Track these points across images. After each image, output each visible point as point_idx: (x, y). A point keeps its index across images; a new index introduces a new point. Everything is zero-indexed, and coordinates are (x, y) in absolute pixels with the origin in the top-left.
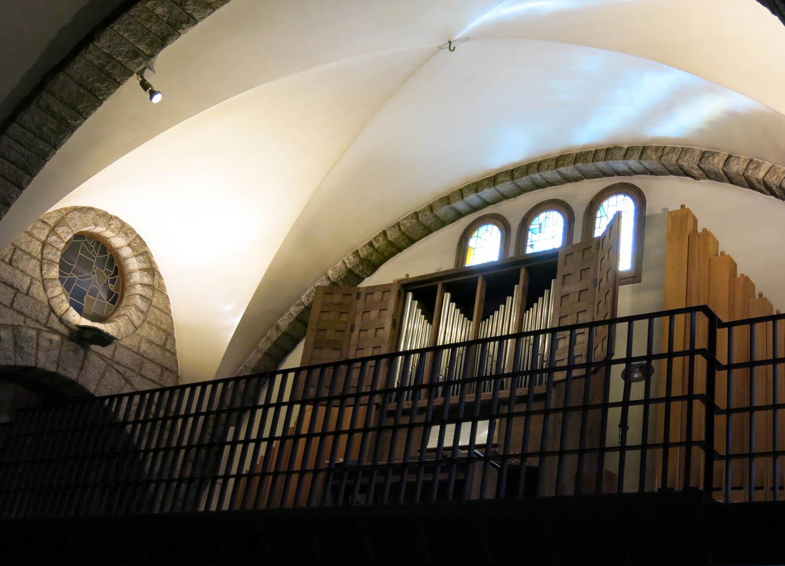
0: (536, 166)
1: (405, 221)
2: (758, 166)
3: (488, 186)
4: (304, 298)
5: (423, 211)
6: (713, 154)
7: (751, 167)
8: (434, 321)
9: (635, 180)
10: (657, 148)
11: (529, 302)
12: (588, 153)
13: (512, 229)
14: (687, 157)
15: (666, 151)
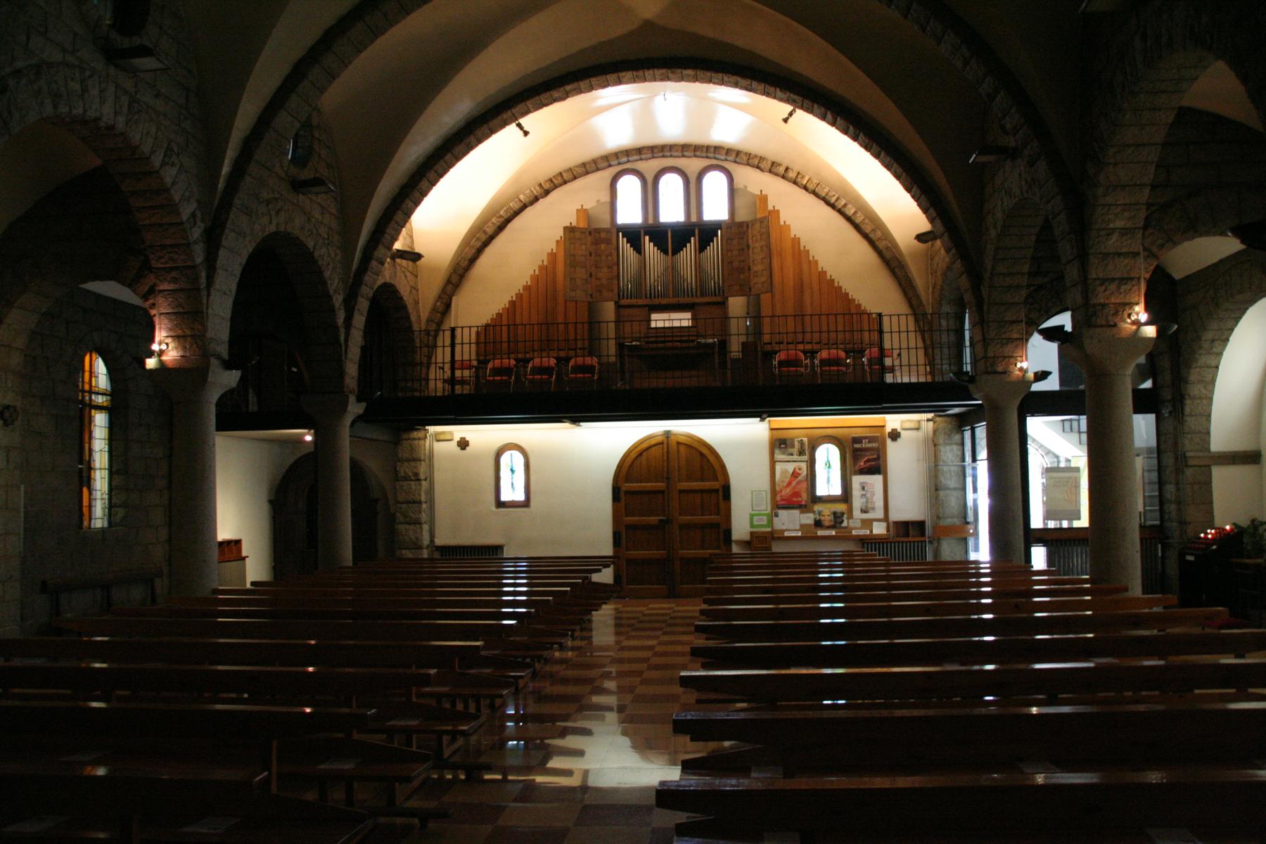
0: (668, 147)
1: (576, 169)
2: (803, 177)
3: (636, 154)
4: (502, 213)
5: (589, 163)
6: (780, 165)
7: (799, 176)
8: (643, 251)
9: (726, 165)
10: (746, 153)
11: (703, 246)
12: (703, 146)
13: (648, 181)
14: (765, 162)
15: (751, 156)
